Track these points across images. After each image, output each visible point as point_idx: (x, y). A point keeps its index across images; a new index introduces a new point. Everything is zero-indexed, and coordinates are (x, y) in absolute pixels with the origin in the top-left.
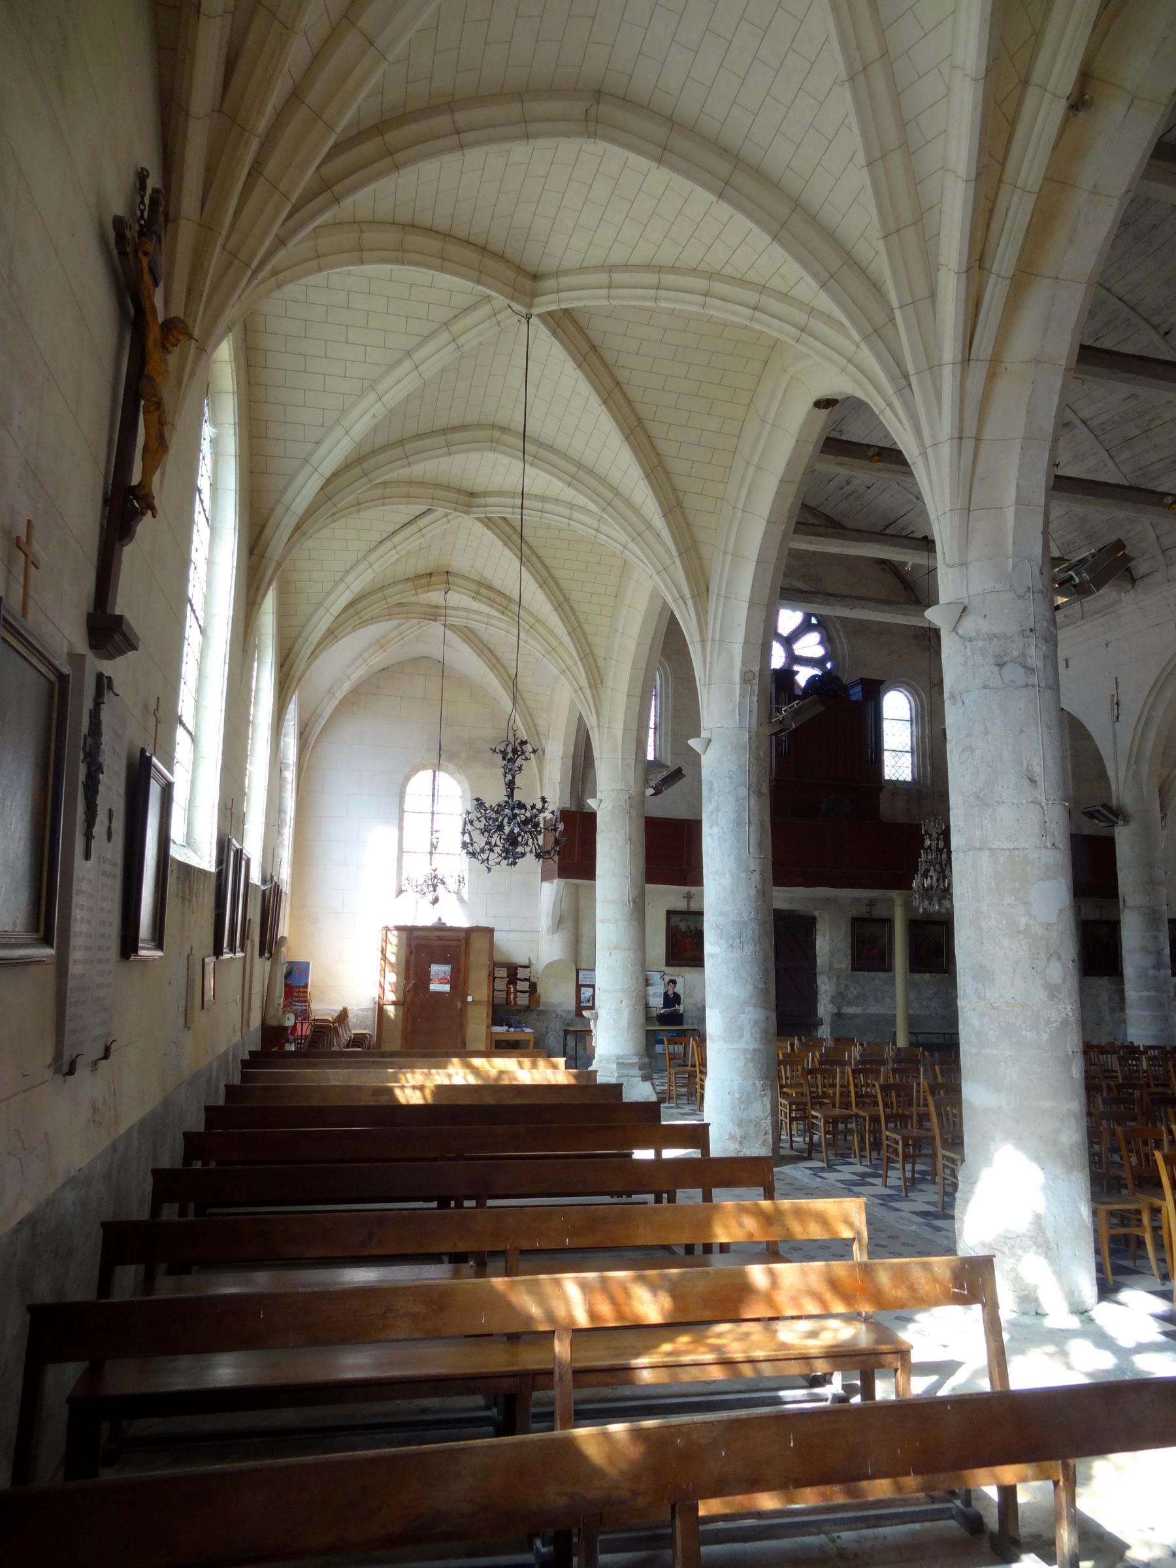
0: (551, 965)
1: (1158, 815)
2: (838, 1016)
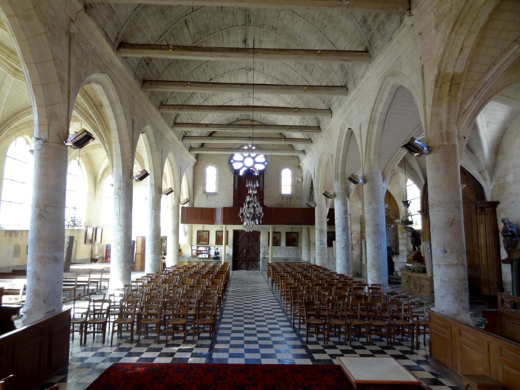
0: (184, 245)
1: (325, 204)
2: (264, 258)
